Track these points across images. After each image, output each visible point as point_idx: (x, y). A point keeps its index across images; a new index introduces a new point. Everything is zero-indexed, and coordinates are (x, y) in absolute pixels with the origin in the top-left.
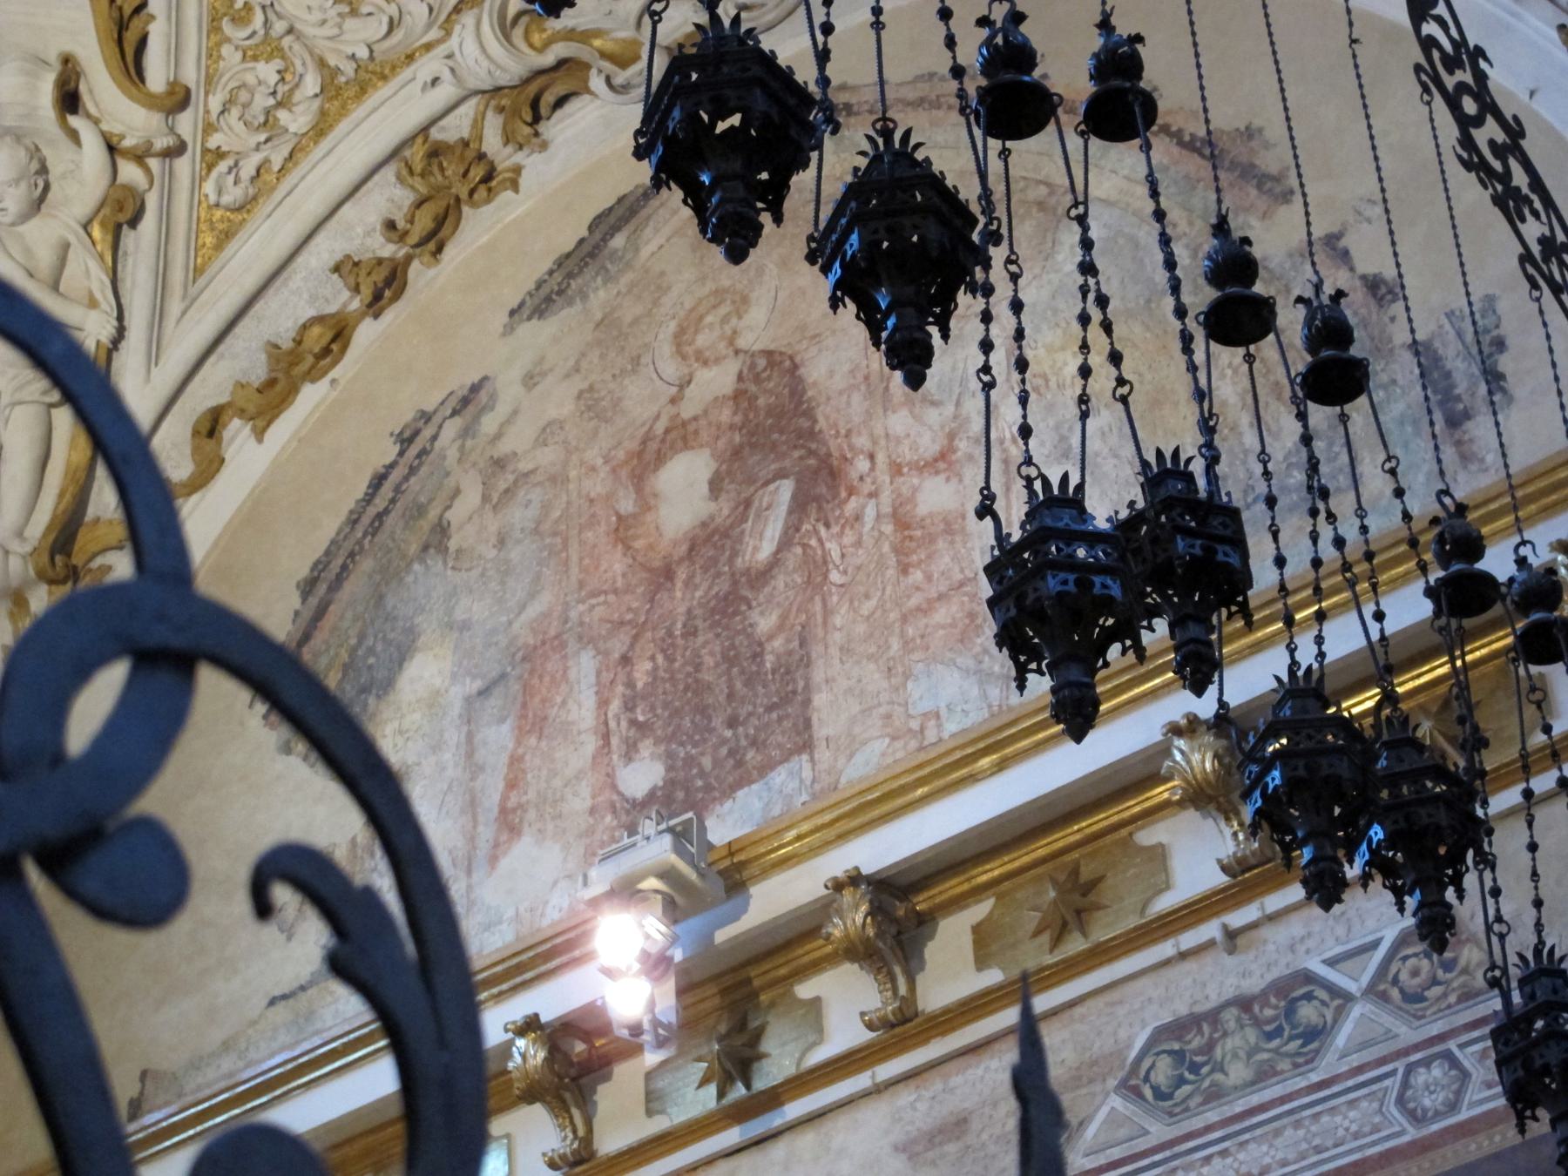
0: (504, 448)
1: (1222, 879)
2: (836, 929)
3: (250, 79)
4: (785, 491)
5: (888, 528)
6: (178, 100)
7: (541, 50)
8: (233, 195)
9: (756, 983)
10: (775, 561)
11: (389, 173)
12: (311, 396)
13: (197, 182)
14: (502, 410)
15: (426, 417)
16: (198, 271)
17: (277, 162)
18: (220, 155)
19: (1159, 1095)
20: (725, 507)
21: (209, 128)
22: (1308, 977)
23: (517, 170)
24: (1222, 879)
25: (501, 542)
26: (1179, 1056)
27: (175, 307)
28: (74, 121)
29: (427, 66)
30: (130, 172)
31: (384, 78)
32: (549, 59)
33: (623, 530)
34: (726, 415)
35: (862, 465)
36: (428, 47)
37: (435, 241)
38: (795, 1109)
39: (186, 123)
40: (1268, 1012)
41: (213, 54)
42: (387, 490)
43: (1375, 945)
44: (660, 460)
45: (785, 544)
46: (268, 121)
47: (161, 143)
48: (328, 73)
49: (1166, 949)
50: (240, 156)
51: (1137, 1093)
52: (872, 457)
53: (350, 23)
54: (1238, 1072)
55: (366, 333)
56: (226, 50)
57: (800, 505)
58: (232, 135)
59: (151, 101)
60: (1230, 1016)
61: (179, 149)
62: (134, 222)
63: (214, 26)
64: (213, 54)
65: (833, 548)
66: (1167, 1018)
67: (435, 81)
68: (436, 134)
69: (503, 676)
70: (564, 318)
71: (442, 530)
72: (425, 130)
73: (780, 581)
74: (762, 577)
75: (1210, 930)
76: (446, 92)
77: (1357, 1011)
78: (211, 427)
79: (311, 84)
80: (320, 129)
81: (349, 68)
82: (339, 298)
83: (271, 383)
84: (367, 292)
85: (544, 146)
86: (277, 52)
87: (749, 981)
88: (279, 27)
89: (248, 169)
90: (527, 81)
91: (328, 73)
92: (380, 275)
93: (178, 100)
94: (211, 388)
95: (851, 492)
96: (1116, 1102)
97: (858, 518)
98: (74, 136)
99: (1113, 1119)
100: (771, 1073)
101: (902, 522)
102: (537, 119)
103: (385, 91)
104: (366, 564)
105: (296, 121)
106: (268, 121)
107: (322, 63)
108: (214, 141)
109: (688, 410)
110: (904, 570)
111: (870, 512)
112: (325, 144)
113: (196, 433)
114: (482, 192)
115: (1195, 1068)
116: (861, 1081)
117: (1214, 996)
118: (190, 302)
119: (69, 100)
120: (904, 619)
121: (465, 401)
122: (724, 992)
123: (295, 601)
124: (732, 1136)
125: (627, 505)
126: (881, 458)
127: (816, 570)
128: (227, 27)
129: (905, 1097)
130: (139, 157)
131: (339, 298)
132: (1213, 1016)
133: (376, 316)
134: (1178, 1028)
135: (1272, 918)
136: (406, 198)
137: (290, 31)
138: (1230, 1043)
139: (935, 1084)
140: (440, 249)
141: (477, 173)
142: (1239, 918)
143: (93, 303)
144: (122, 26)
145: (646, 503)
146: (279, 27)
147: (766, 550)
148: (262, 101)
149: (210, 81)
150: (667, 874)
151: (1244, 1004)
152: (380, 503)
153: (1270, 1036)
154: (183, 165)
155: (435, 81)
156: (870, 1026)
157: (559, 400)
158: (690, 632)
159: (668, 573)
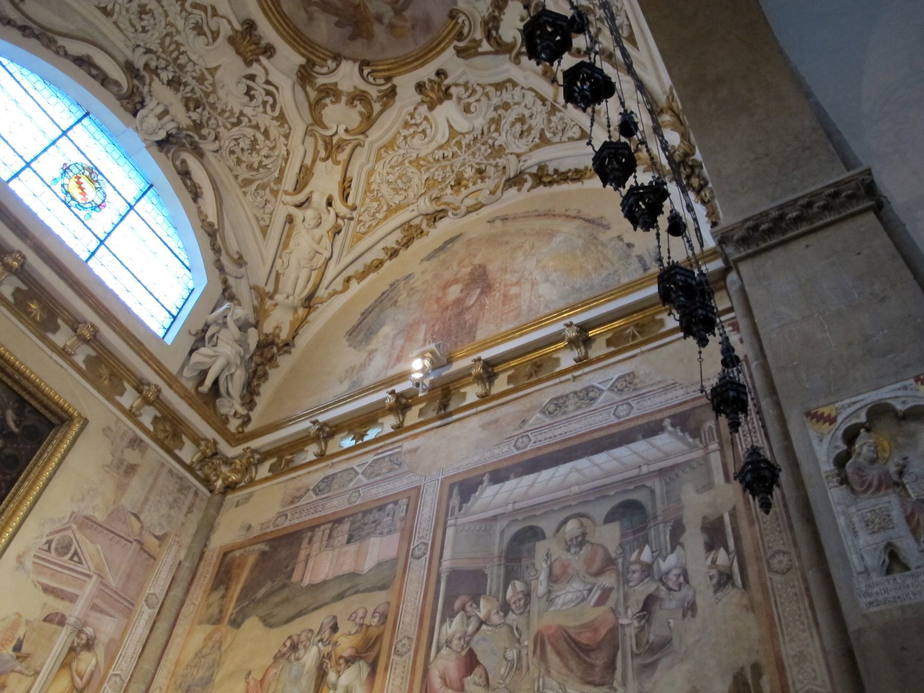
0: (414, 286)
1: (574, 363)
2: (473, 372)
3: (371, 206)
4: (478, 291)
5: (502, 297)
6: (354, 208)
7: (439, 206)
8: (363, 230)
9: (451, 388)
10: (473, 305)
11: (399, 231)
12: (372, 276)
13: (355, 227)
14: (415, 279)
15: (397, 281)
16: (352, 246)
17: (374, 224)
18: (361, 221)
19: (550, 413)
20: (463, 295)
21: (360, 215)
22: (593, 387)
23: (428, 232)
24: (574, 363)
25: (409, 303)
26: (556, 405)
27: (345, 253)
28: (329, 208)
29: (411, 208)
30: (340, 221)
31: (402, 209)
32: (440, 208)
33: (438, 300)
34: (467, 277)
35: (498, 285)
36: (413, 204)
37: (406, 245)
38: (455, 417)
39: (355, 214)
40: (581, 395)
41: (364, 199)
42: (385, 295)
43: (611, 379)
44: (450, 286)
45: (476, 301)
46: (373, 216)
47: (348, 216)
48: (389, 206)
49: (557, 380)
50: (366, 222)
51: (544, 413)
52: (500, 284)
53: (396, 196)
54: (571, 408)
55: (388, 264)
56: (367, 199)
57: (481, 294)
58: (365, 217)
59: (348, 207)
60: (571, 396)
61: (351, 219)
62: (339, 232)
63: (365, 193)
64: (364, 199)
65: (487, 302)
66: (554, 396)
67: (413, 210)
68: (412, 223)
69: (403, 330)
70: (434, 261)
71: (396, 302)
72: (409, 221)
73: (473, 309)
74: (469, 308)
75: (569, 376)
76: (415, 213)
77: (605, 394)
78: (348, 280)
79: (385, 208)
80: (385, 218)
81: (394, 206)
82: (383, 256)
83: (364, 272)
84: (389, 254)
85: (435, 227)
86: (379, 200)
87: (449, 387)
88: (380, 195)
89: (367, 225)
90: (434, 213)
91: (389, 206)
92: (393, 251)
93: (354, 208)
94: (350, 272)
95: (494, 290)
96: (539, 415)
97: (495, 295)
98: (329, 212)
99: (537, 419)
100: (451, 408)
101: (505, 296)
102: (435, 221)
103: (401, 212)
104: (377, 309)
105: (380, 216)
106: (373, 216)
107: (388, 204)
108: (361, 218)
109: (458, 276)
110: (504, 305)
111: (498, 294)
112: (386, 222)
113: (344, 281)
114: (419, 236)
115: (560, 407)
116: (474, 411)
117: (568, 391)
118: (348, 253)
119: (329, 204)
120: (502, 315)
121: (407, 277)
122: (443, 390)
123: (359, 316)
124: (439, 423)
125: (440, 295)
126: (502, 283)
127: (483, 306)
128: (368, 194)
129: (484, 415)
130: (343, 218)
131: (383, 256)
132: (567, 396)
133: (391, 260)
134: (557, 398)
135: (586, 374)
136: (402, 236)
137: (382, 196)
138: (570, 402)
139: (492, 412)
140: (407, 247)
141: (419, 231)
142: (576, 374)
143: (326, 249)
144: (344, 190)
145: (444, 295)
146: (380, 195)
147: (472, 302)
148: (373, 210)
149: (362, 205)
150: (432, 353)
151: (575, 393)
152: (383, 298)
153: (581, 400)
154: (352, 223)
155: (413, 210)
156: (478, 396)
157: (428, 276)
158: (450, 319)
159: (447, 308)
